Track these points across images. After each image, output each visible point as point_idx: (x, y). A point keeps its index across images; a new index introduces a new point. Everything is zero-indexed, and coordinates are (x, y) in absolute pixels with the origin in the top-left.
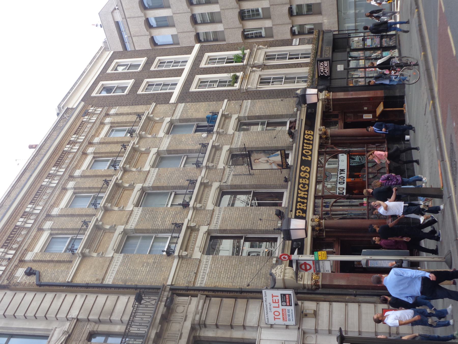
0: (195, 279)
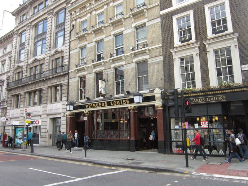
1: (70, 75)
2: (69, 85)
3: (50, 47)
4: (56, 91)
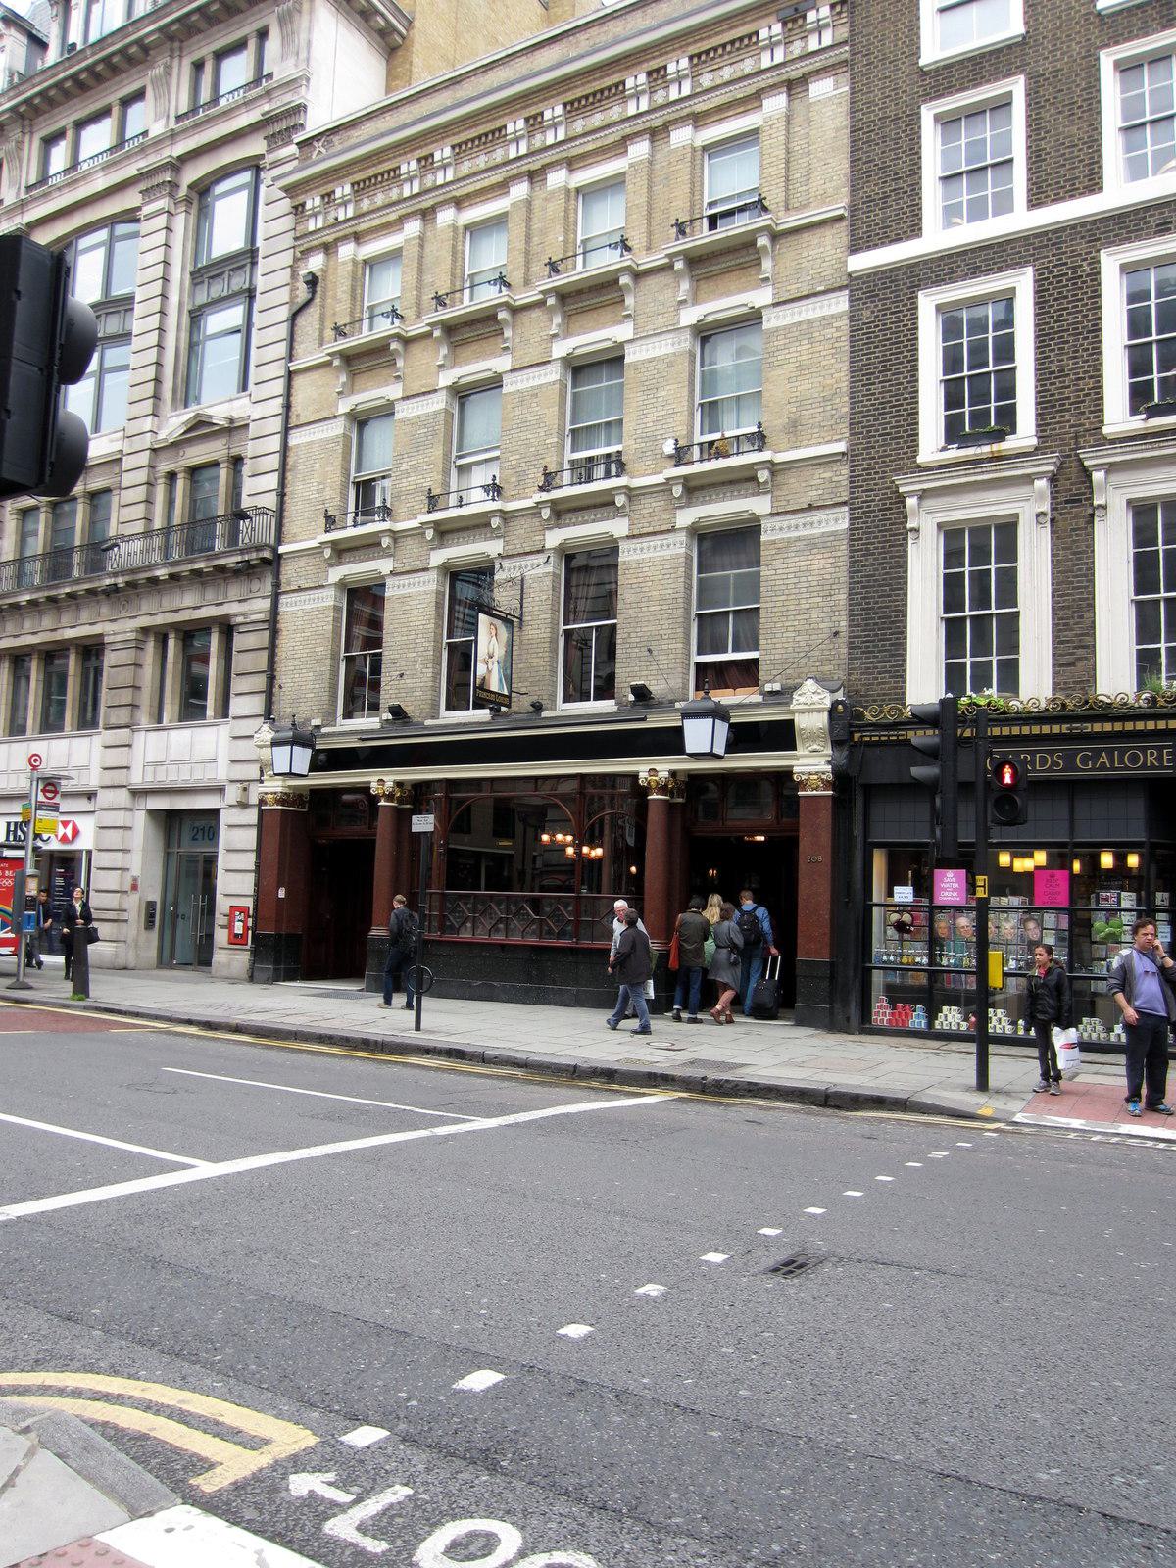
0: (293, 591)
1: (289, 572)
2: (281, 626)
3: (156, 396)
4: (194, 658)
